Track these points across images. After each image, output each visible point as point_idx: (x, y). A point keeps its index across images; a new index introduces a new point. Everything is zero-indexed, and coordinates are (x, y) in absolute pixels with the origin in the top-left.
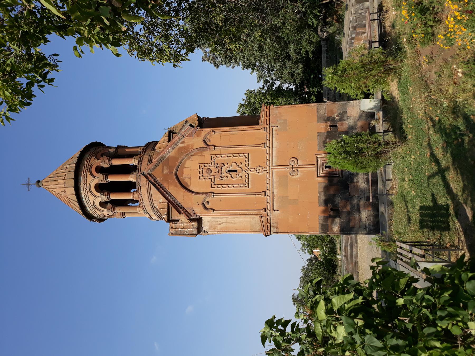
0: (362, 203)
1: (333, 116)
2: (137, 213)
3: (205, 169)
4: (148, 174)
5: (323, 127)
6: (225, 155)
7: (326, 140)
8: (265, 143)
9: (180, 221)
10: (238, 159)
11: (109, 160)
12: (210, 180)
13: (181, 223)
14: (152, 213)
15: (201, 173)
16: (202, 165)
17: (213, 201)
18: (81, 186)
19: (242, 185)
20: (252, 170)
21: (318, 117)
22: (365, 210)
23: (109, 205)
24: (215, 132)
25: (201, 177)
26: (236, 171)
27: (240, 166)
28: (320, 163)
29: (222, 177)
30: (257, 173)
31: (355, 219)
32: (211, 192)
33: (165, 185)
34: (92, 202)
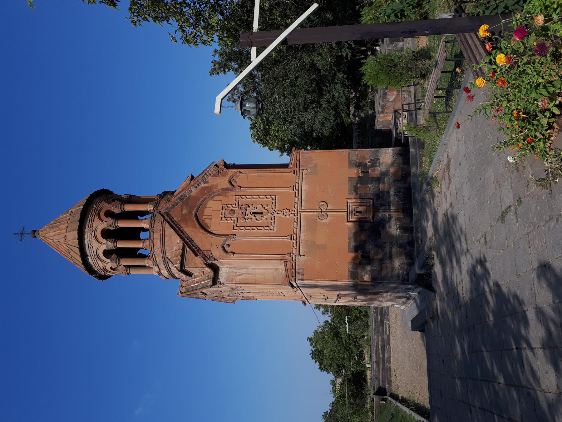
0: (394, 250)
1: (365, 162)
2: (145, 267)
3: (228, 210)
4: (165, 213)
5: (354, 173)
9: (193, 276)
10: (264, 200)
11: (121, 204)
12: (232, 221)
13: (194, 278)
14: (162, 266)
15: (223, 214)
18: (86, 230)
19: (266, 228)
21: (349, 163)
22: (398, 257)
23: (114, 256)
26: (262, 213)
27: (266, 208)
28: (350, 209)
31: (387, 267)
33: (183, 225)
34: (95, 249)
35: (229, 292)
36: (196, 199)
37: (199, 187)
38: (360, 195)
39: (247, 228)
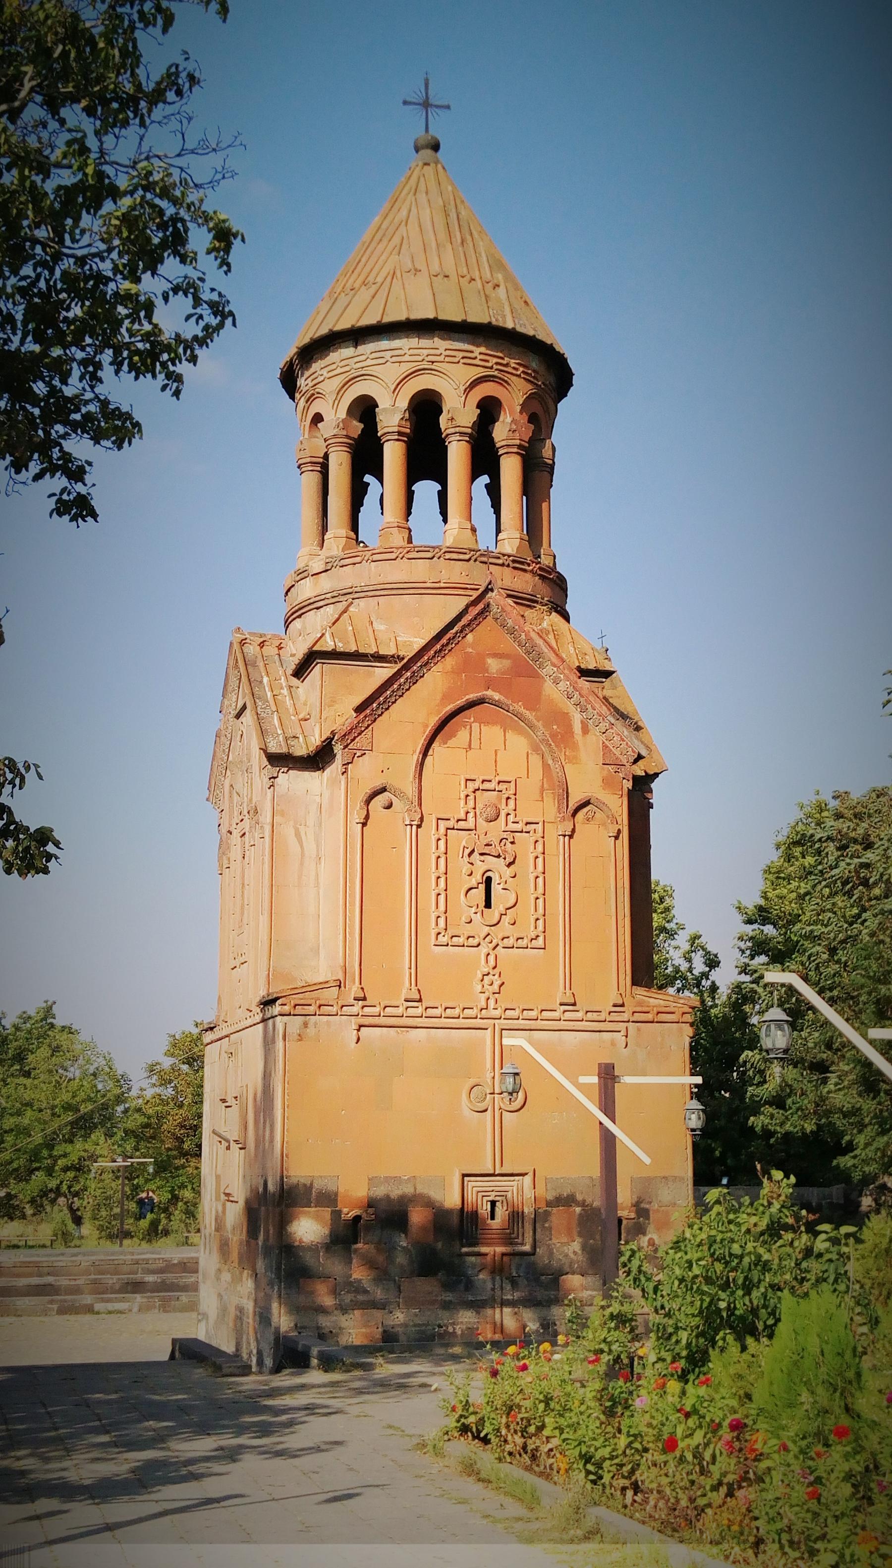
4: (488, 605)
6: (540, 868)
7: (578, 1204)
8: (574, 1004)
15: (486, 786)
16: (508, 789)
17: (391, 823)
20: (492, 959)
23: (357, 427)
24: (616, 838)
25: (471, 786)
26: (488, 905)
27: (506, 920)
29: (470, 855)
30: (480, 976)
32: (422, 819)
33: (449, 662)
35: (245, 792)
36: (533, 700)
37: (569, 707)
38: (547, 1214)
39: (442, 861)
